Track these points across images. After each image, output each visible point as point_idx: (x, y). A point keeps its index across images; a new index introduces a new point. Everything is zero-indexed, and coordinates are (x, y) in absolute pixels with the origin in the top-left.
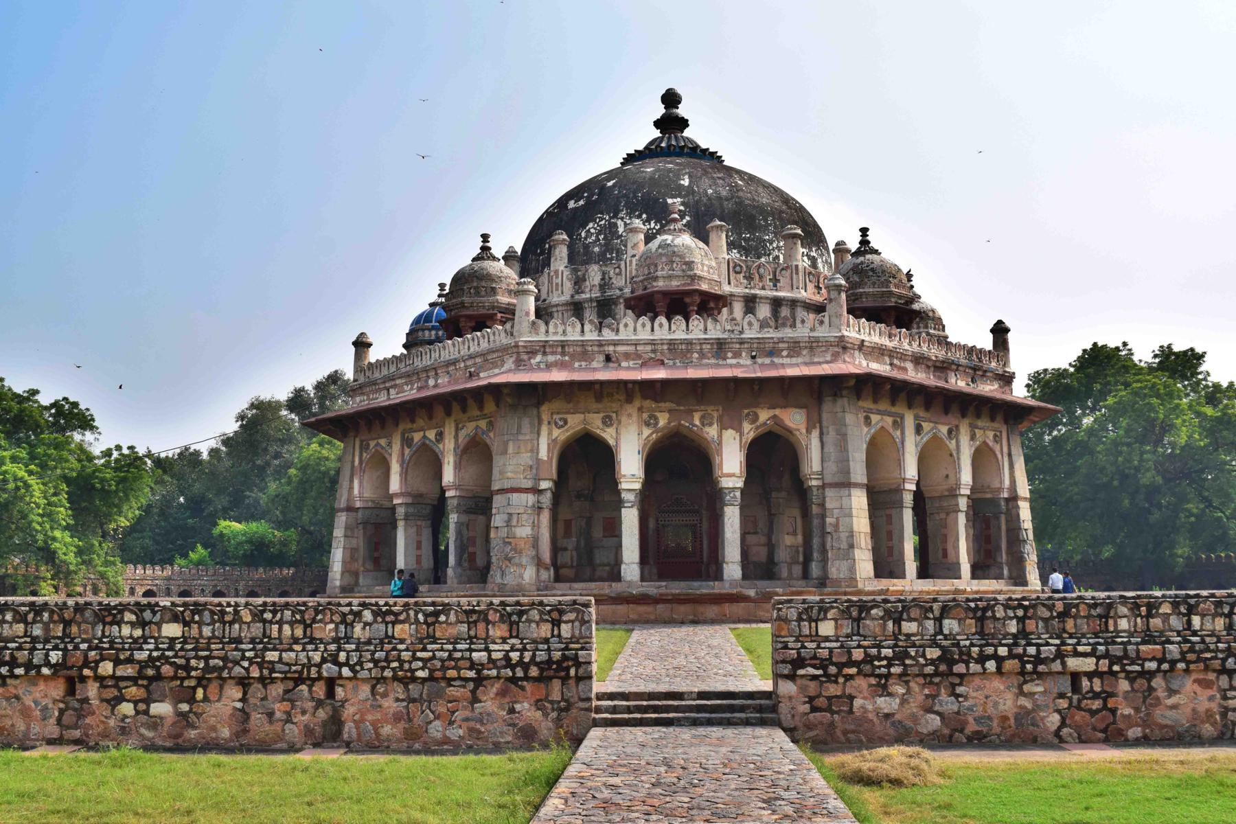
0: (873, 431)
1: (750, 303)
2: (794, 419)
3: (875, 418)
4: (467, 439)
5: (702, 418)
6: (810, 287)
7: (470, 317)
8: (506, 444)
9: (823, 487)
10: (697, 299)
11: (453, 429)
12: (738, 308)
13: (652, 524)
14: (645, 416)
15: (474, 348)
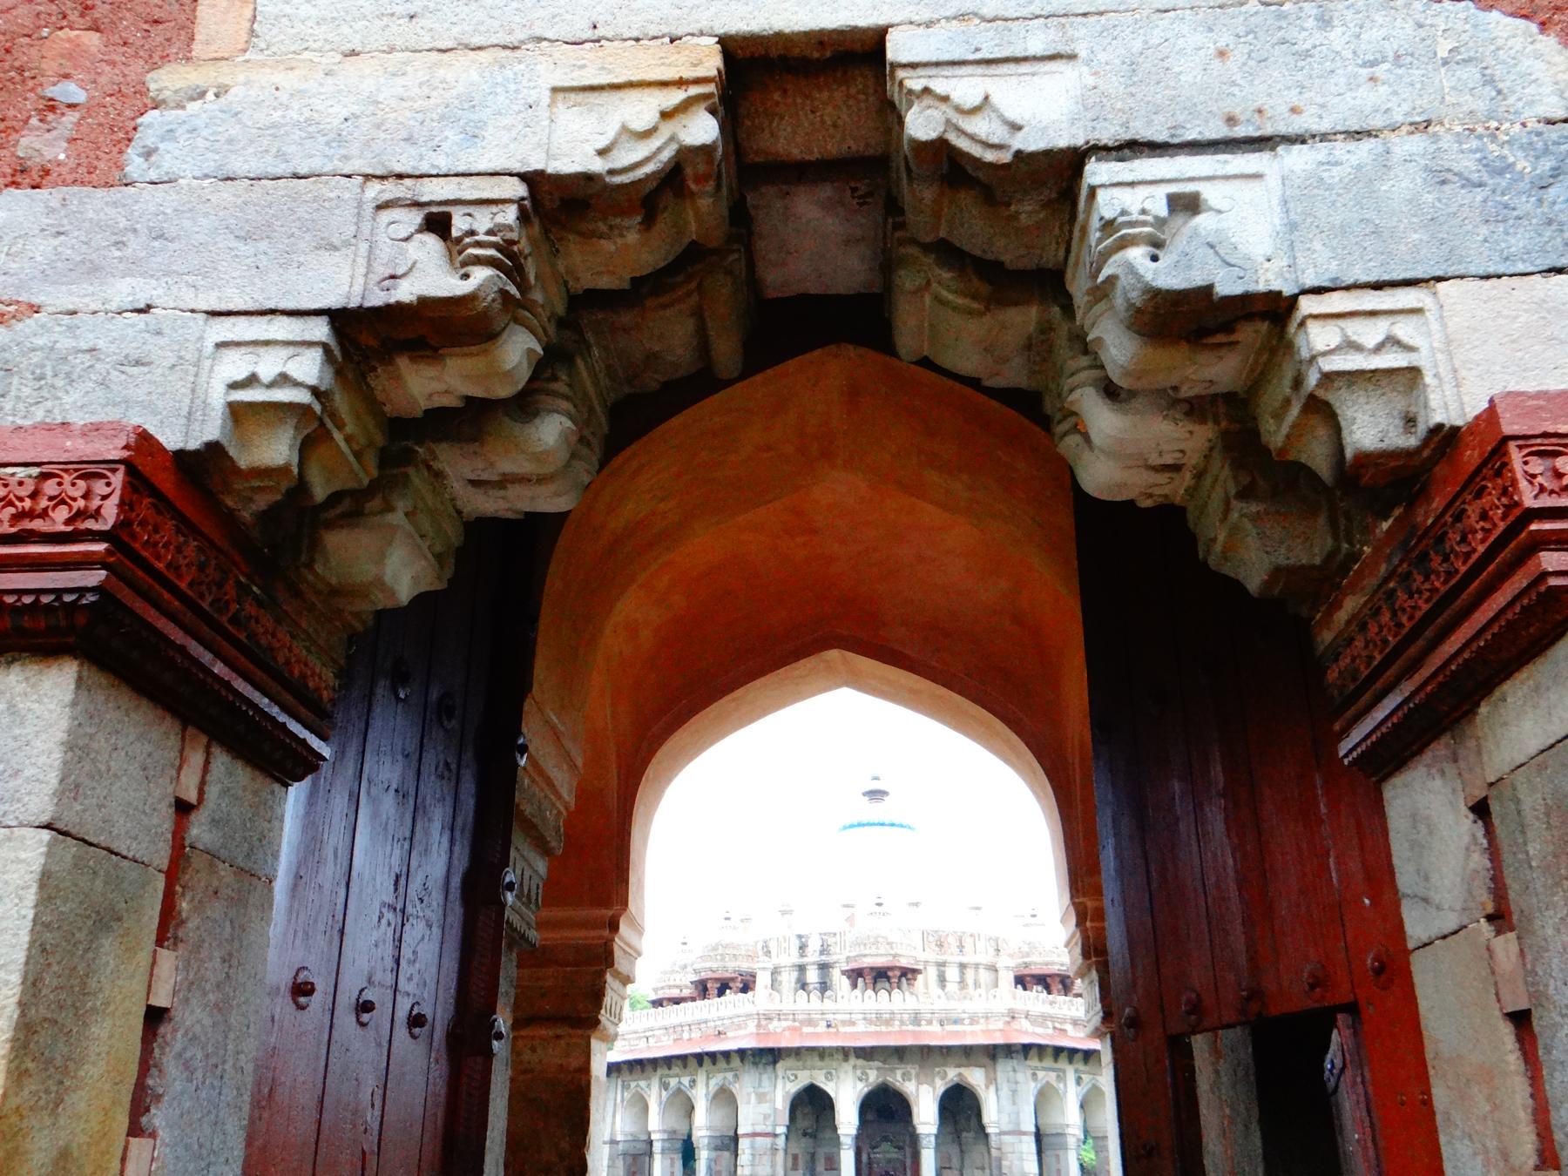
0: (1039, 1086)
1: (941, 965)
2: (975, 1077)
3: (1041, 1074)
4: (716, 1088)
5: (904, 1074)
6: (992, 951)
7: (716, 980)
8: (749, 1094)
9: (1002, 1133)
10: (898, 973)
11: (705, 1077)
12: (932, 973)
13: (864, 1158)
14: (859, 1072)
15: (723, 1012)
